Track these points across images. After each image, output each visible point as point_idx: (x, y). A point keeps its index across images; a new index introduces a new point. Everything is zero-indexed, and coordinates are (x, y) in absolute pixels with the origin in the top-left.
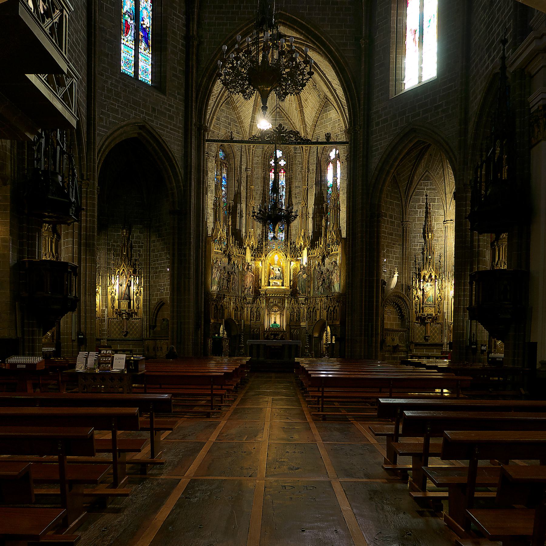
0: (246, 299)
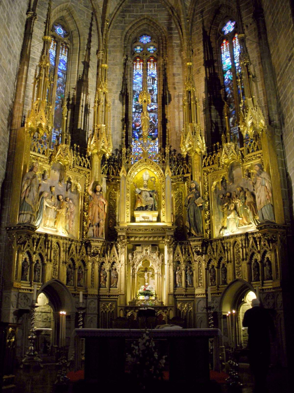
0: (91, 247)
